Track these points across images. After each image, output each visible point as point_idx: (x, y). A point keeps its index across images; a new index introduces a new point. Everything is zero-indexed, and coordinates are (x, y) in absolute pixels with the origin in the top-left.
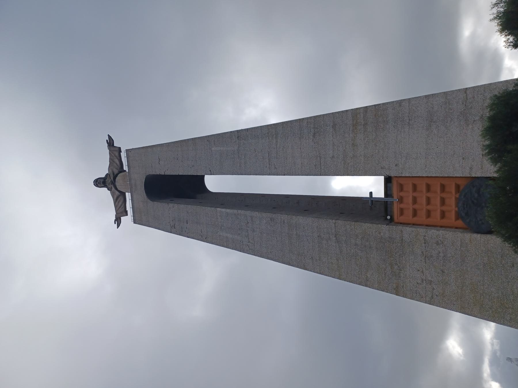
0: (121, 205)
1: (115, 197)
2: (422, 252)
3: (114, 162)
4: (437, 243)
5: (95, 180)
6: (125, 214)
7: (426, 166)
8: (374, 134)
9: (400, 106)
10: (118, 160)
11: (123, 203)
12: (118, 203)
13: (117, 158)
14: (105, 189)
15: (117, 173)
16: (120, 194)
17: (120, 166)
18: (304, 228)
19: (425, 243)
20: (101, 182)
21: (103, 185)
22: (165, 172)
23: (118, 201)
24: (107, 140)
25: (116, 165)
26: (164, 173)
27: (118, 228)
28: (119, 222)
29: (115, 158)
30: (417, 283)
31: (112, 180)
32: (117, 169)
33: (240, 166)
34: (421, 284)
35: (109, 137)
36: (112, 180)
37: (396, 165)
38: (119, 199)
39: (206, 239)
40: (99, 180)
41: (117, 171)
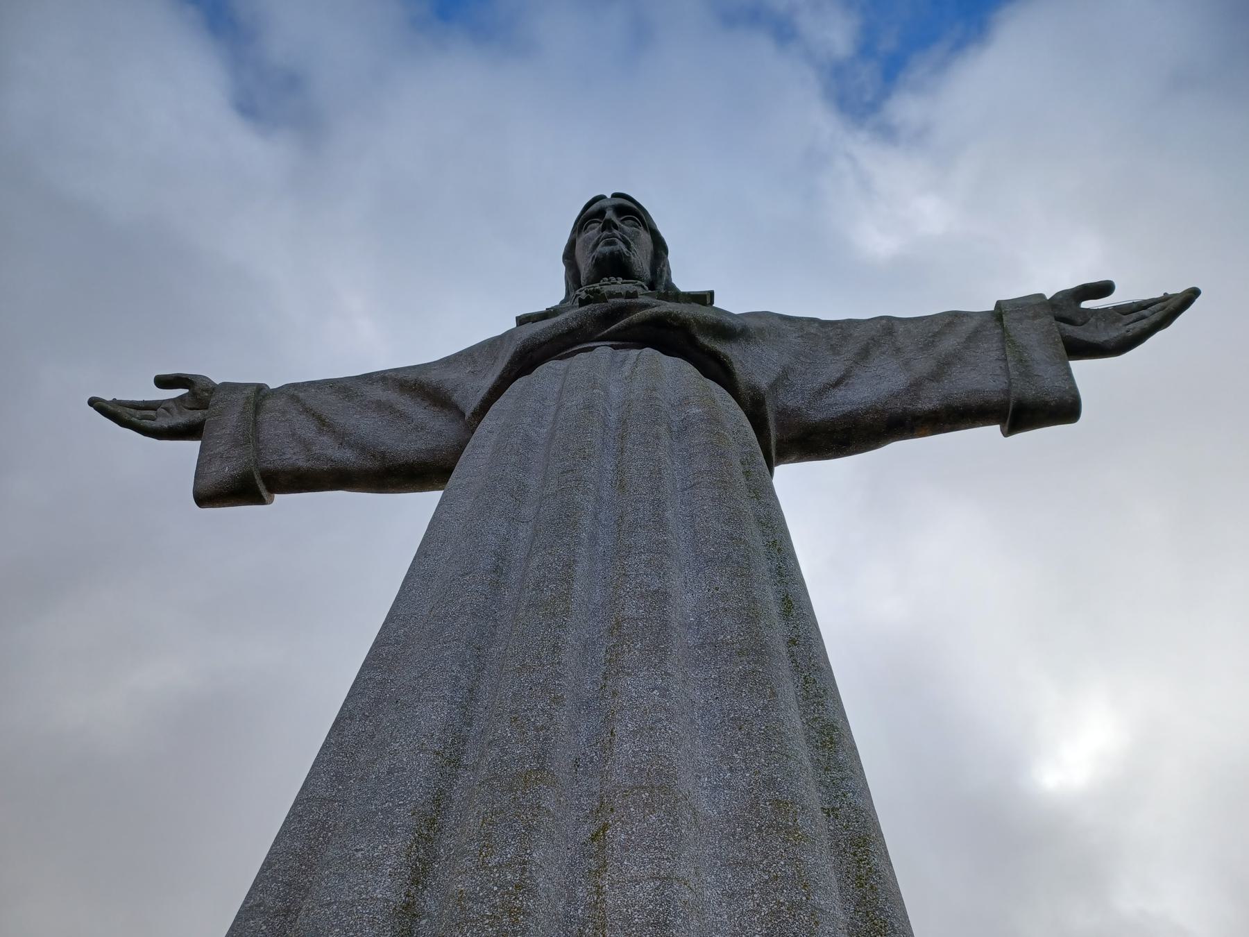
0: (342, 438)
1: (450, 377)
3: (864, 354)
6: (225, 470)
10: (895, 395)
11: (363, 449)
12: (380, 406)
13: (916, 386)
15: (738, 368)
16: (468, 414)
17: (816, 416)
20: (621, 246)
23: (404, 403)
24: (1104, 289)
25: (833, 370)
27: (94, 403)
28: (163, 422)
29: (923, 365)
31: (646, 306)
32: (773, 386)
36: (646, 306)
38: (420, 412)
40: (645, 237)
41: (763, 382)
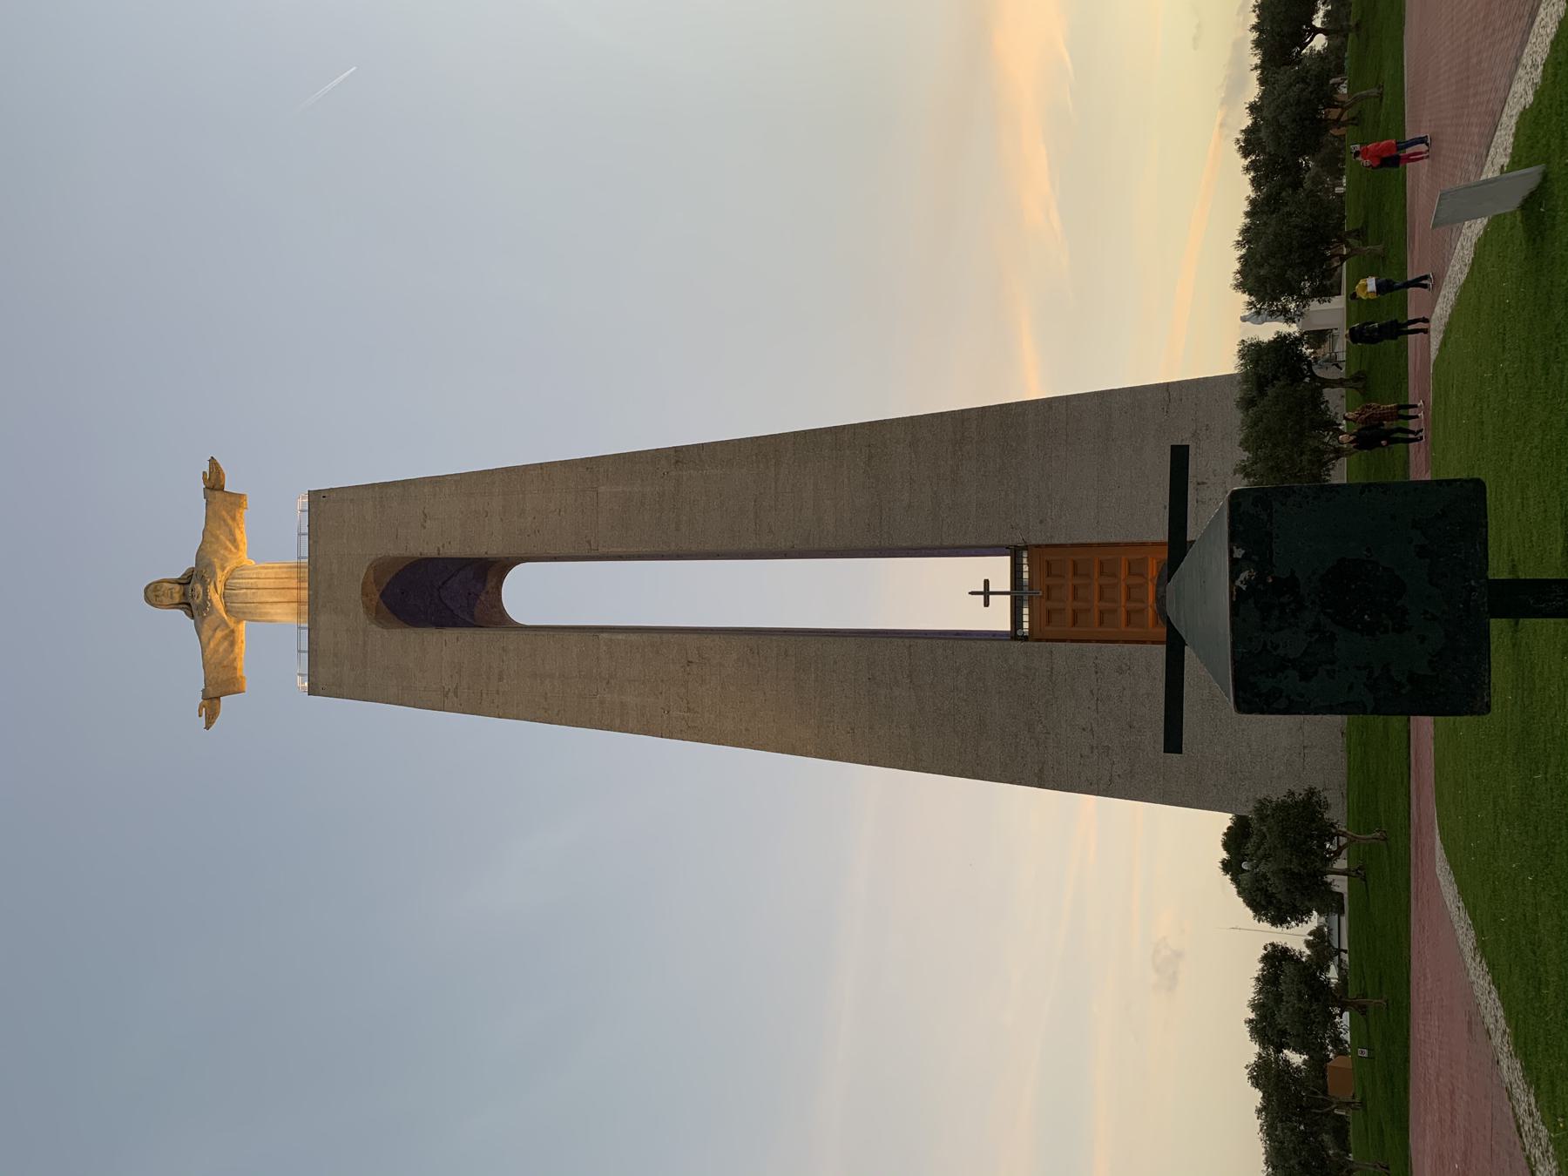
2: (1091, 691)
4: (1120, 671)
5: (150, 585)
7: (1098, 522)
8: (998, 460)
9: (1051, 408)
14: (180, 614)
18: (835, 663)
19: (1097, 673)
21: (177, 601)
22: (441, 549)
24: (204, 473)
26: (439, 550)
27: (207, 728)
30: (1081, 756)
33: (677, 529)
34: (1088, 757)
35: (212, 461)
37: (1041, 522)
39: (558, 715)
